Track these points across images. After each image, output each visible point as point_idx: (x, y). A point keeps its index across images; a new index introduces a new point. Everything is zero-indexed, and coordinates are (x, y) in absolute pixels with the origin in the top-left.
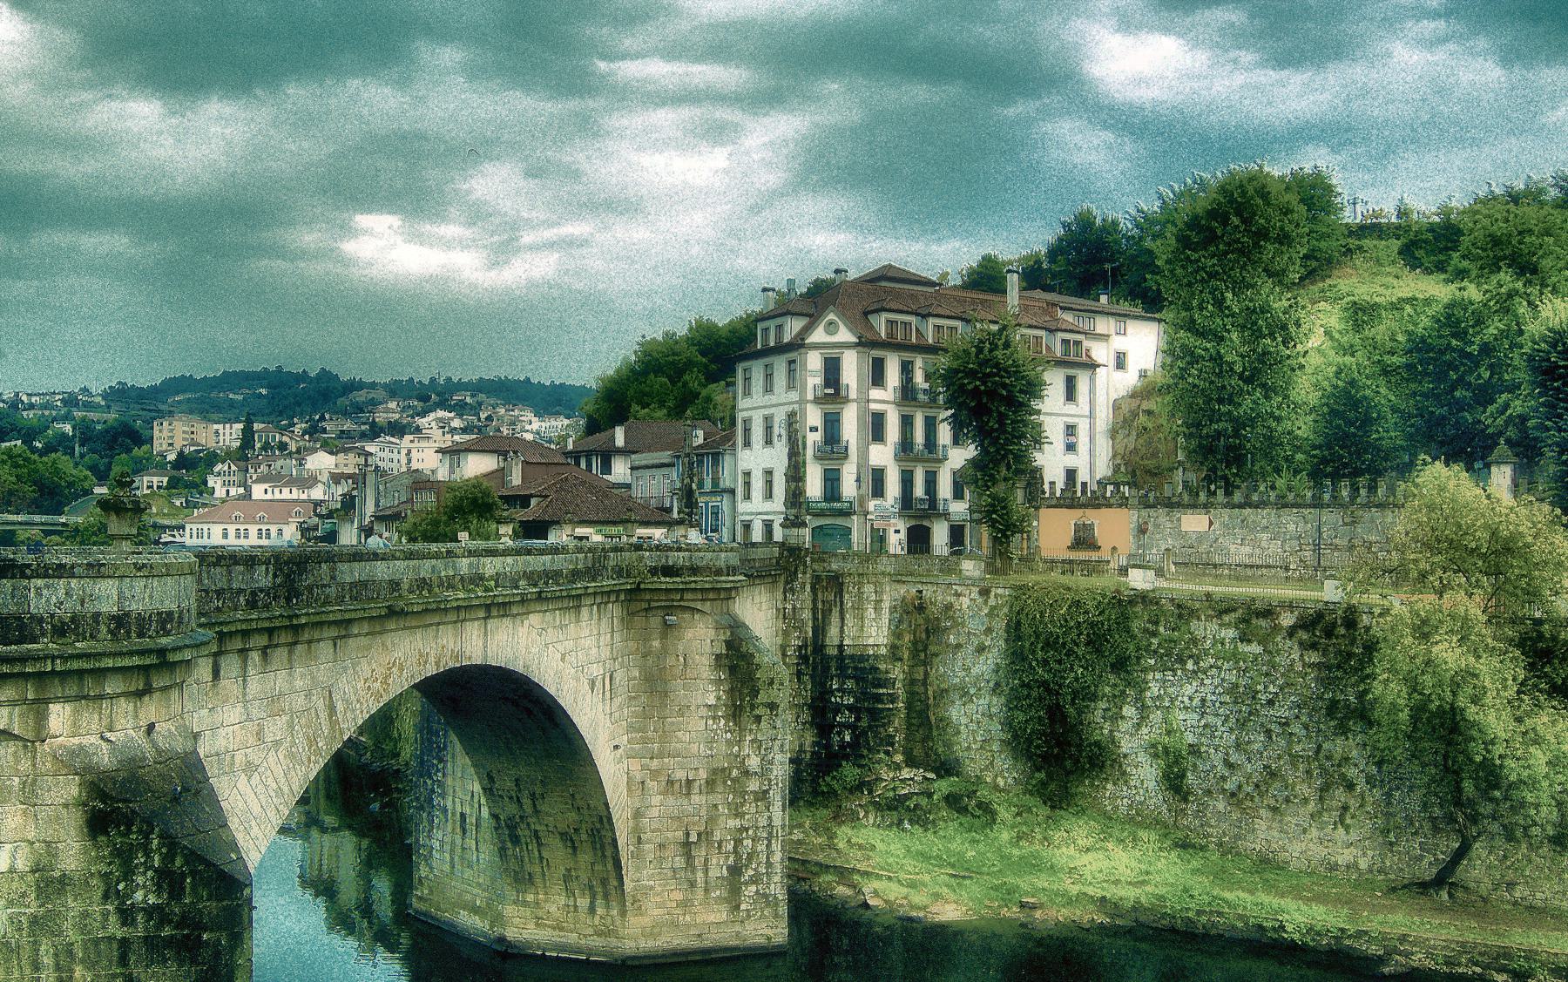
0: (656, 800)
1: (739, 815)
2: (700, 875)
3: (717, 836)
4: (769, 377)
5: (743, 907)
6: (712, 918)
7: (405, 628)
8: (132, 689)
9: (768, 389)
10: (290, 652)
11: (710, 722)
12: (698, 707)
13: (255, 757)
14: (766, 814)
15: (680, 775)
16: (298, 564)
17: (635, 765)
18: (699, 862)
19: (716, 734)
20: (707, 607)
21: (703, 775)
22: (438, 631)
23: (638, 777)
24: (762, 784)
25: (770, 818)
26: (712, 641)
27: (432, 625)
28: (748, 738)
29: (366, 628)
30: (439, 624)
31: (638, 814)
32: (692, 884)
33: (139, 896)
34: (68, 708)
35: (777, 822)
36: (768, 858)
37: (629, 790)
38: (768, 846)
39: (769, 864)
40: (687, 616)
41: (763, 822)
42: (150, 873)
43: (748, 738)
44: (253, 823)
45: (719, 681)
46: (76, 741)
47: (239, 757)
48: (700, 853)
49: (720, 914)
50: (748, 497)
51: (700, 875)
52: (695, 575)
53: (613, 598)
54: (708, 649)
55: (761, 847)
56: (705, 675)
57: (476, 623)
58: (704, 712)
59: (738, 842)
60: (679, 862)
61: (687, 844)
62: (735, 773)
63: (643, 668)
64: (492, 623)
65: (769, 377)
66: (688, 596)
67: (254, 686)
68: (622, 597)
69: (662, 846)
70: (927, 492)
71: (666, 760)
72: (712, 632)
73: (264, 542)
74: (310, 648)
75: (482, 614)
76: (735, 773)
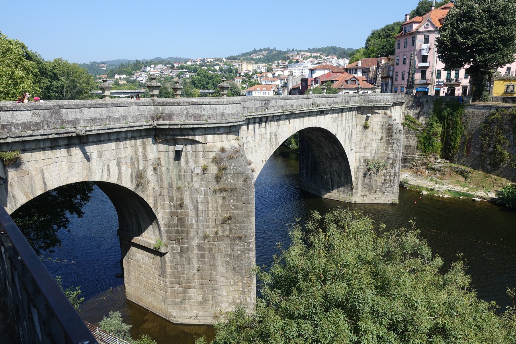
1: (386, 169)
4: (406, 43)
5: (386, 193)
8: (226, 131)
9: (405, 46)
11: (379, 144)
16: (267, 100)
17: (357, 154)
24: (393, 161)
25: (395, 170)
28: (390, 148)
33: (229, 180)
34: (212, 136)
35: (397, 171)
36: (394, 181)
37: (355, 161)
38: (394, 178)
41: (393, 171)
42: (231, 175)
43: (390, 148)
45: (382, 132)
46: (214, 144)
50: (396, 80)
52: (377, 103)
53: (353, 109)
54: (379, 123)
55: (392, 178)
56: (378, 131)
58: (377, 141)
59: (385, 176)
62: (385, 158)
65: (406, 43)
68: (355, 109)
70: (456, 77)
72: (381, 119)
73: (265, 95)
76: (385, 158)
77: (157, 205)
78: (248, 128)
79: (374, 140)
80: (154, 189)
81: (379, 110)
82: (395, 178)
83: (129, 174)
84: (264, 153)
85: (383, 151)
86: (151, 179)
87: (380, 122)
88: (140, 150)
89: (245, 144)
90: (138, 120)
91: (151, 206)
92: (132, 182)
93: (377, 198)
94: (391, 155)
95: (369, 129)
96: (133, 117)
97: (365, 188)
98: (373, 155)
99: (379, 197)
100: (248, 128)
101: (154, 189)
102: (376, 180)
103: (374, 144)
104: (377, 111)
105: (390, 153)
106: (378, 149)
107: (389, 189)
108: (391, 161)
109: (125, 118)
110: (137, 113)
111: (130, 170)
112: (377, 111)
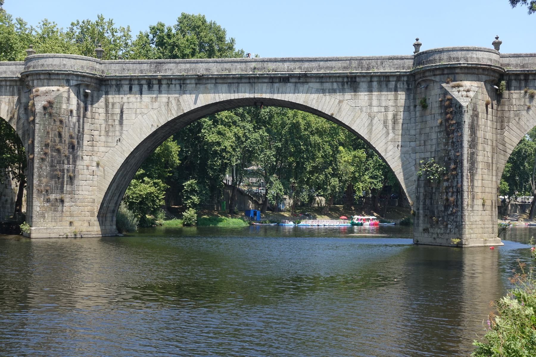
7: (216, 83)
10: (159, 86)
11: (439, 134)
12: (435, 127)
13: (145, 111)
19: (440, 140)
22: (238, 86)
26: (439, 95)
27: (233, 83)
28: (450, 141)
29: (193, 81)
30: (238, 83)
34: (37, 81)
44: (144, 127)
47: (138, 111)
57: (266, 84)
58: (437, 129)
64: (276, 85)
71: (426, 153)
74: (169, 87)
75: (266, 80)
77: (25, 137)
79: (434, 128)
80: (23, 124)
81: (434, 75)
82: (459, 196)
83: (6, 111)
84: (155, 117)
85: (443, 147)
86: (22, 117)
87: (438, 95)
89: (126, 104)
90: (15, 74)
91: (20, 136)
92: (7, 115)
93: (440, 236)
95: (428, 111)
96: (11, 72)
97: (426, 215)
99: (442, 234)
101: (23, 124)
102: (438, 202)
103: (434, 136)
104: (433, 78)
105: (451, 150)
106: (438, 144)
107: (452, 218)
109: (5, 72)
110: (14, 70)
111: (7, 107)
112: (433, 78)
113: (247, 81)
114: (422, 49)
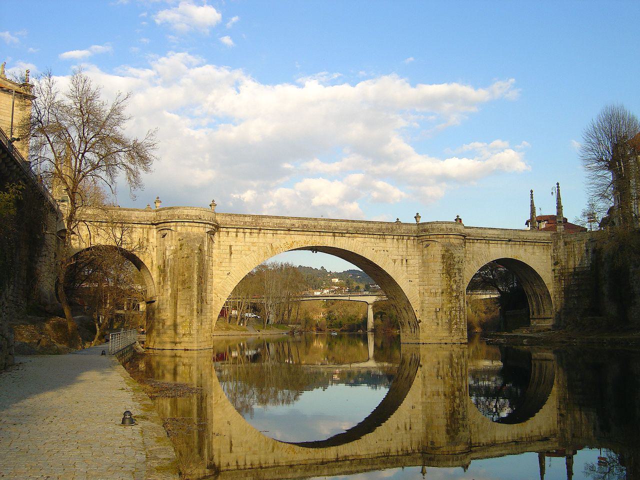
0: (427, 298)
2: (440, 321)
3: (445, 309)
6: (444, 335)
13: (248, 252)
14: (459, 303)
15: (433, 291)
17: (422, 288)
18: (439, 317)
20: (439, 240)
21: (440, 291)
23: (422, 292)
31: (422, 302)
32: (438, 324)
39: (460, 319)
40: (434, 243)
48: (440, 314)
49: (446, 334)
51: (440, 321)
54: (440, 253)
55: (457, 314)
58: (439, 272)
60: (434, 317)
61: (436, 312)
63: (423, 260)
66: (432, 237)
67: (247, 239)
69: (429, 312)
78: (237, 236)
88: (145, 236)
94: (454, 287)
98: (437, 287)
100: (237, 236)
108: (454, 294)
112: (436, 240)
113: (318, 234)
114: (421, 221)
